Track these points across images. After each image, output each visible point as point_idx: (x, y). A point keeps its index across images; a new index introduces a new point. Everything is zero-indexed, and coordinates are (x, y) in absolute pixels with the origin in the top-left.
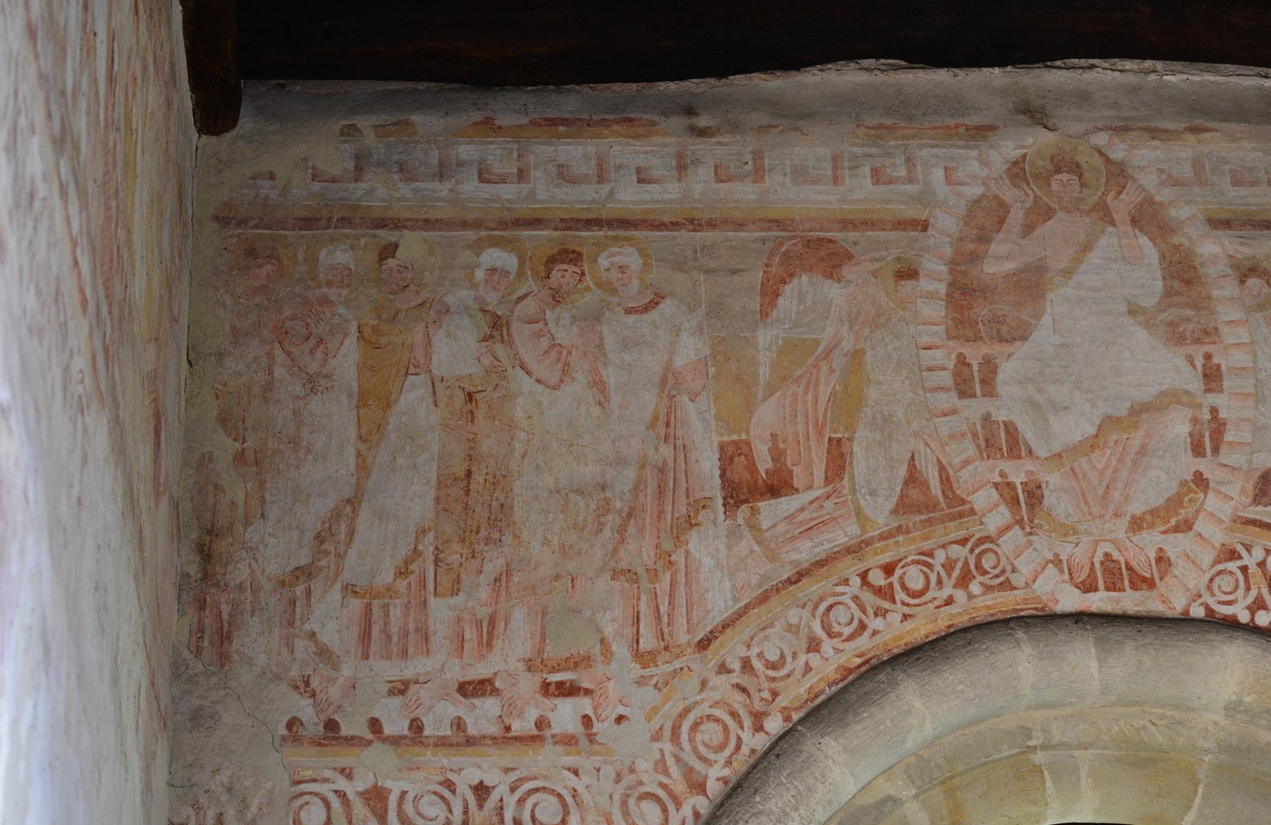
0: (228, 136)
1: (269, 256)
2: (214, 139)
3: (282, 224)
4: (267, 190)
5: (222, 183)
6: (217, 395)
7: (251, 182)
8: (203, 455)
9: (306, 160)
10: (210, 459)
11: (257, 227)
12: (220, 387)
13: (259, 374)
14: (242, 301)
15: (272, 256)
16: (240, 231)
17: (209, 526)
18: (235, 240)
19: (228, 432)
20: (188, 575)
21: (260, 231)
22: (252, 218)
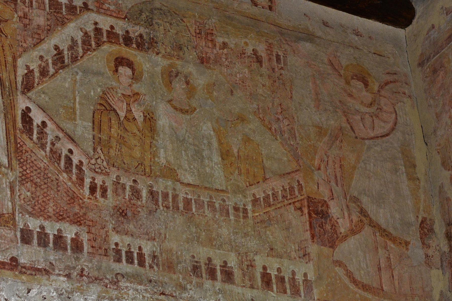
0: (415, 21)
1: (441, 68)
2: (410, 27)
3: (442, 48)
4: (434, 35)
5: (417, 46)
6: (438, 152)
7: (427, 36)
8: (440, 187)
9: (442, 8)
10: (443, 187)
11: (434, 56)
12: (439, 148)
13: (449, 130)
14: (436, 98)
15: (442, 66)
16: (429, 64)
17: (448, 222)
18: (428, 69)
19: (445, 169)
20: (445, 252)
21: (435, 58)
22: (431, 54)
